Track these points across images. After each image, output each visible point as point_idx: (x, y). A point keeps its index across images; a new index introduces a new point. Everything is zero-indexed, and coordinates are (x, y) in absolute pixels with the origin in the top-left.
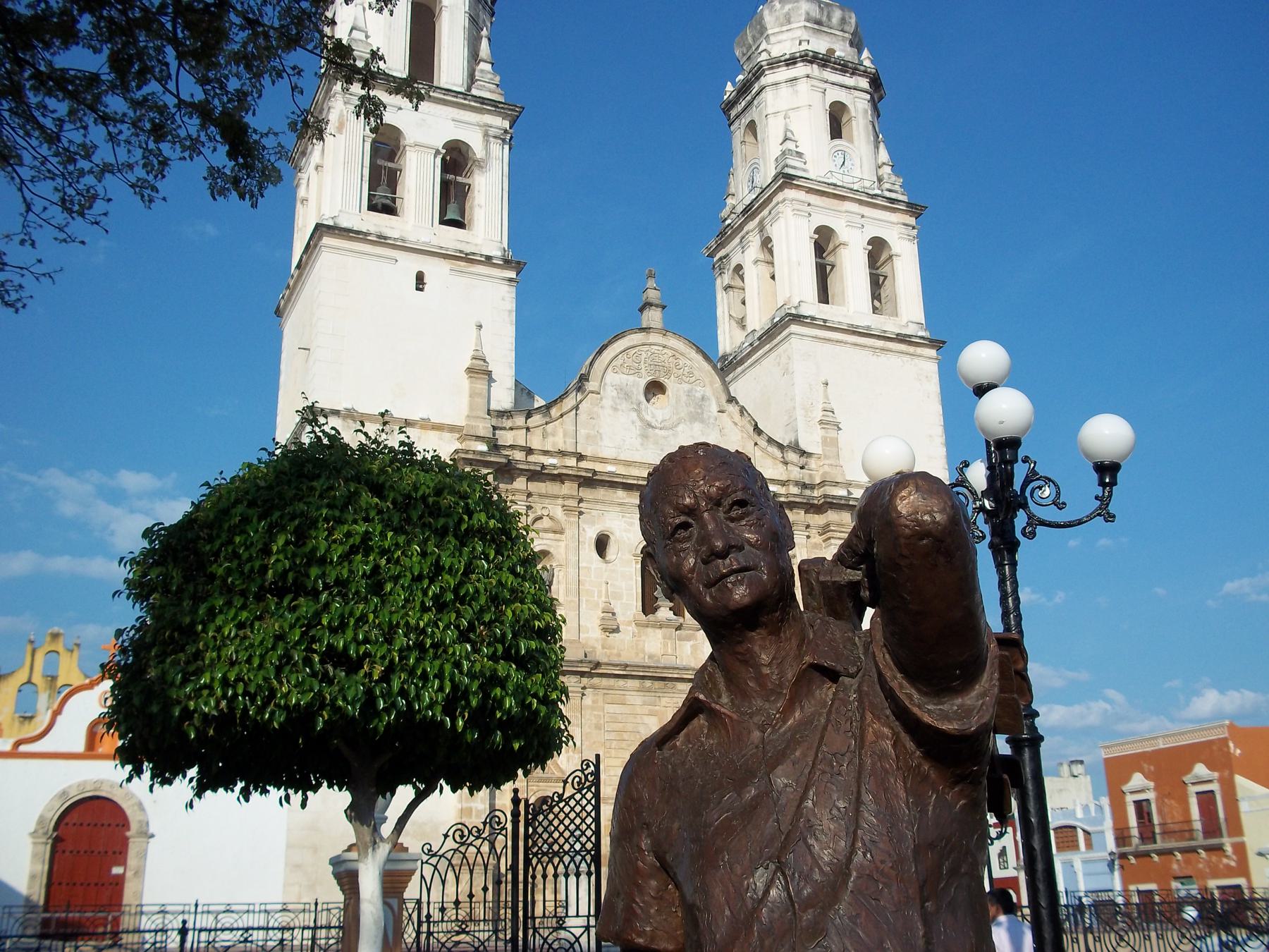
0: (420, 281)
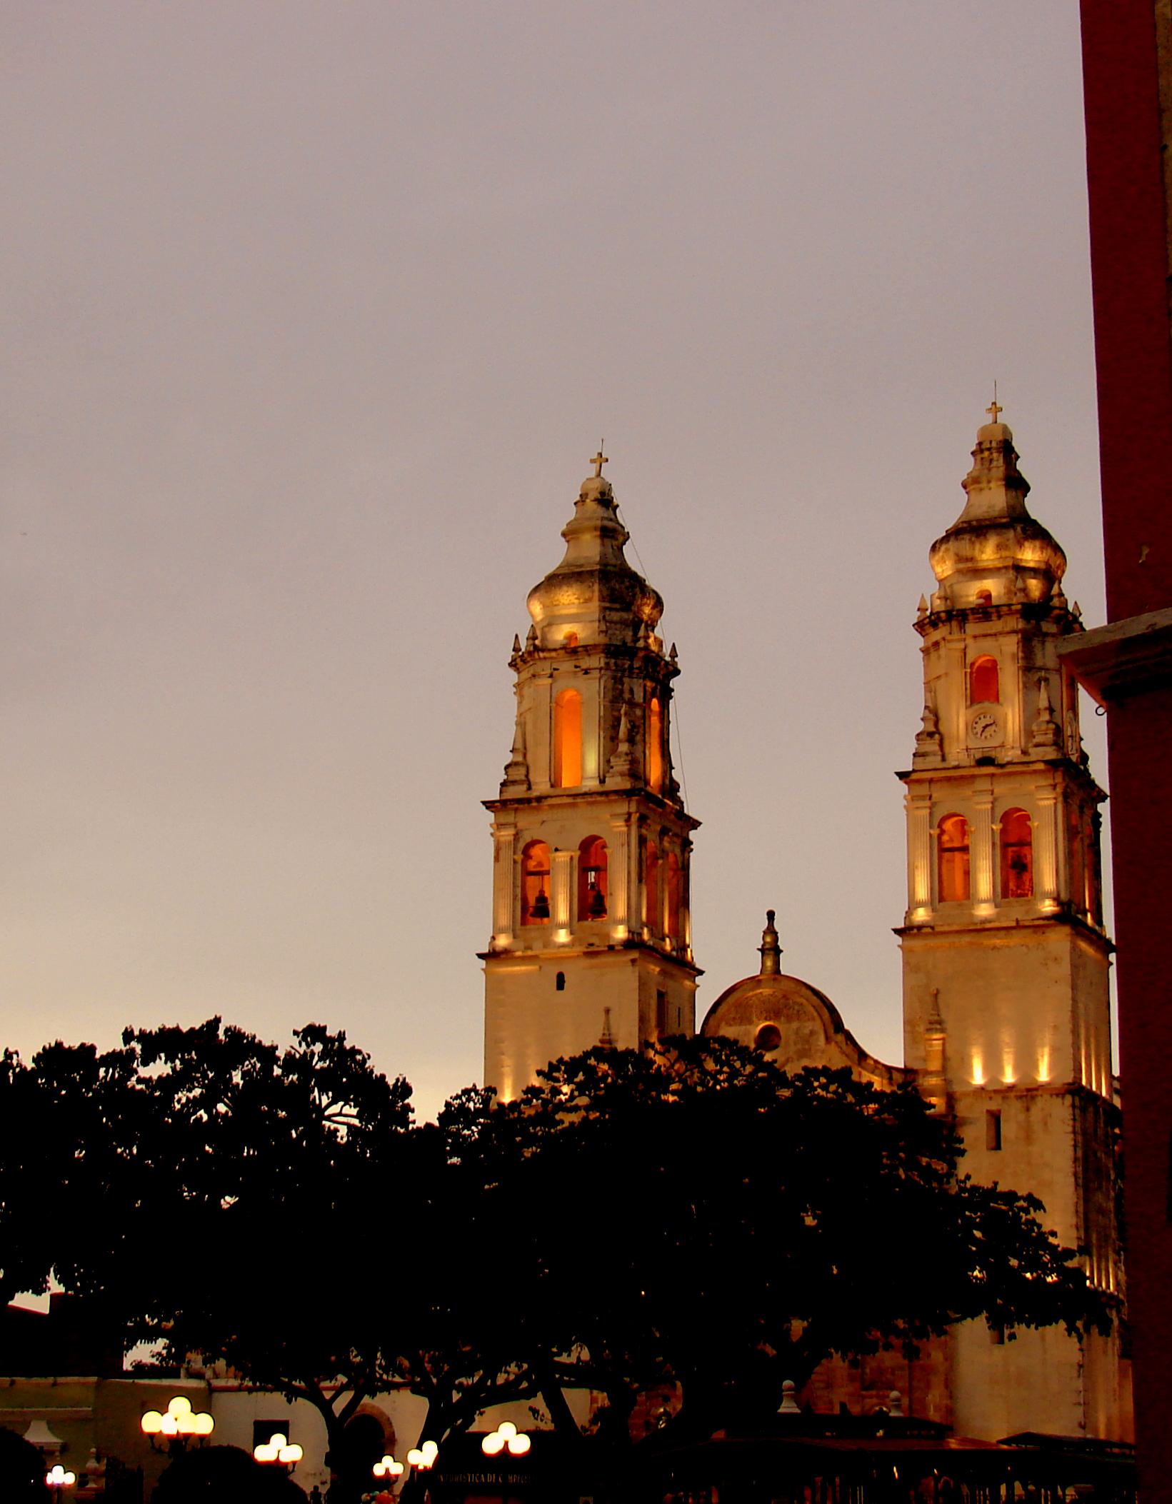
0: (561, 982)
